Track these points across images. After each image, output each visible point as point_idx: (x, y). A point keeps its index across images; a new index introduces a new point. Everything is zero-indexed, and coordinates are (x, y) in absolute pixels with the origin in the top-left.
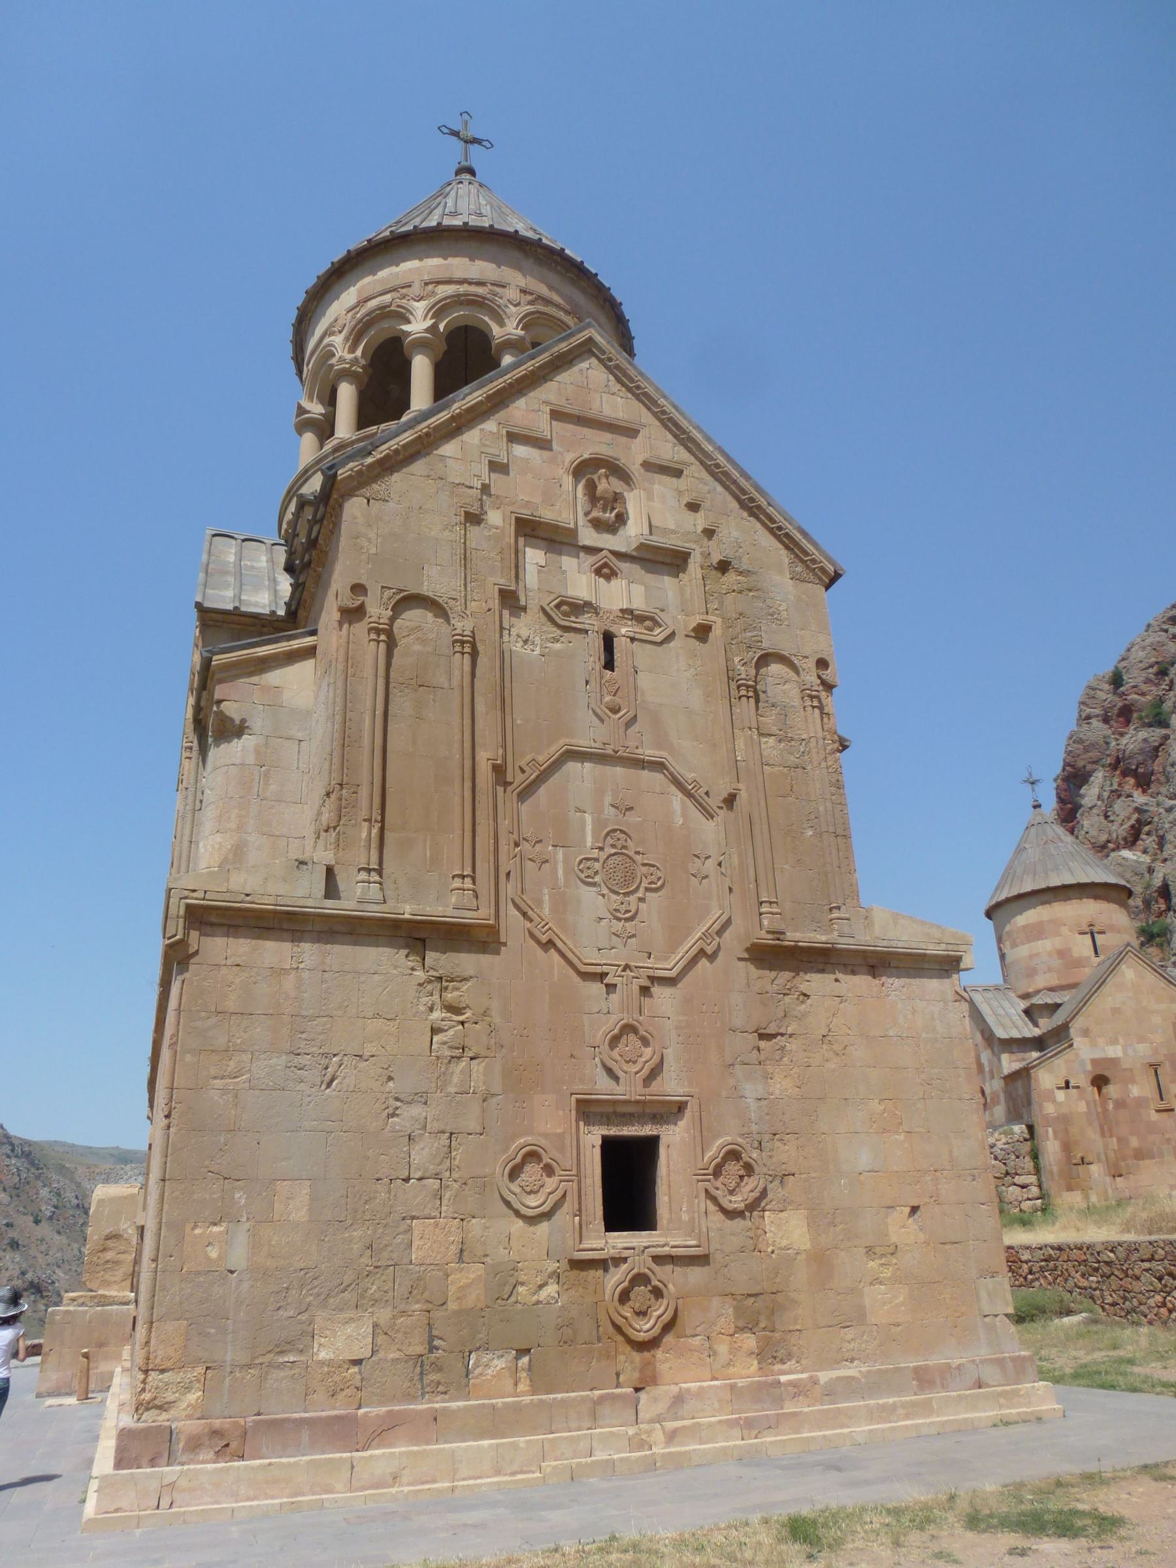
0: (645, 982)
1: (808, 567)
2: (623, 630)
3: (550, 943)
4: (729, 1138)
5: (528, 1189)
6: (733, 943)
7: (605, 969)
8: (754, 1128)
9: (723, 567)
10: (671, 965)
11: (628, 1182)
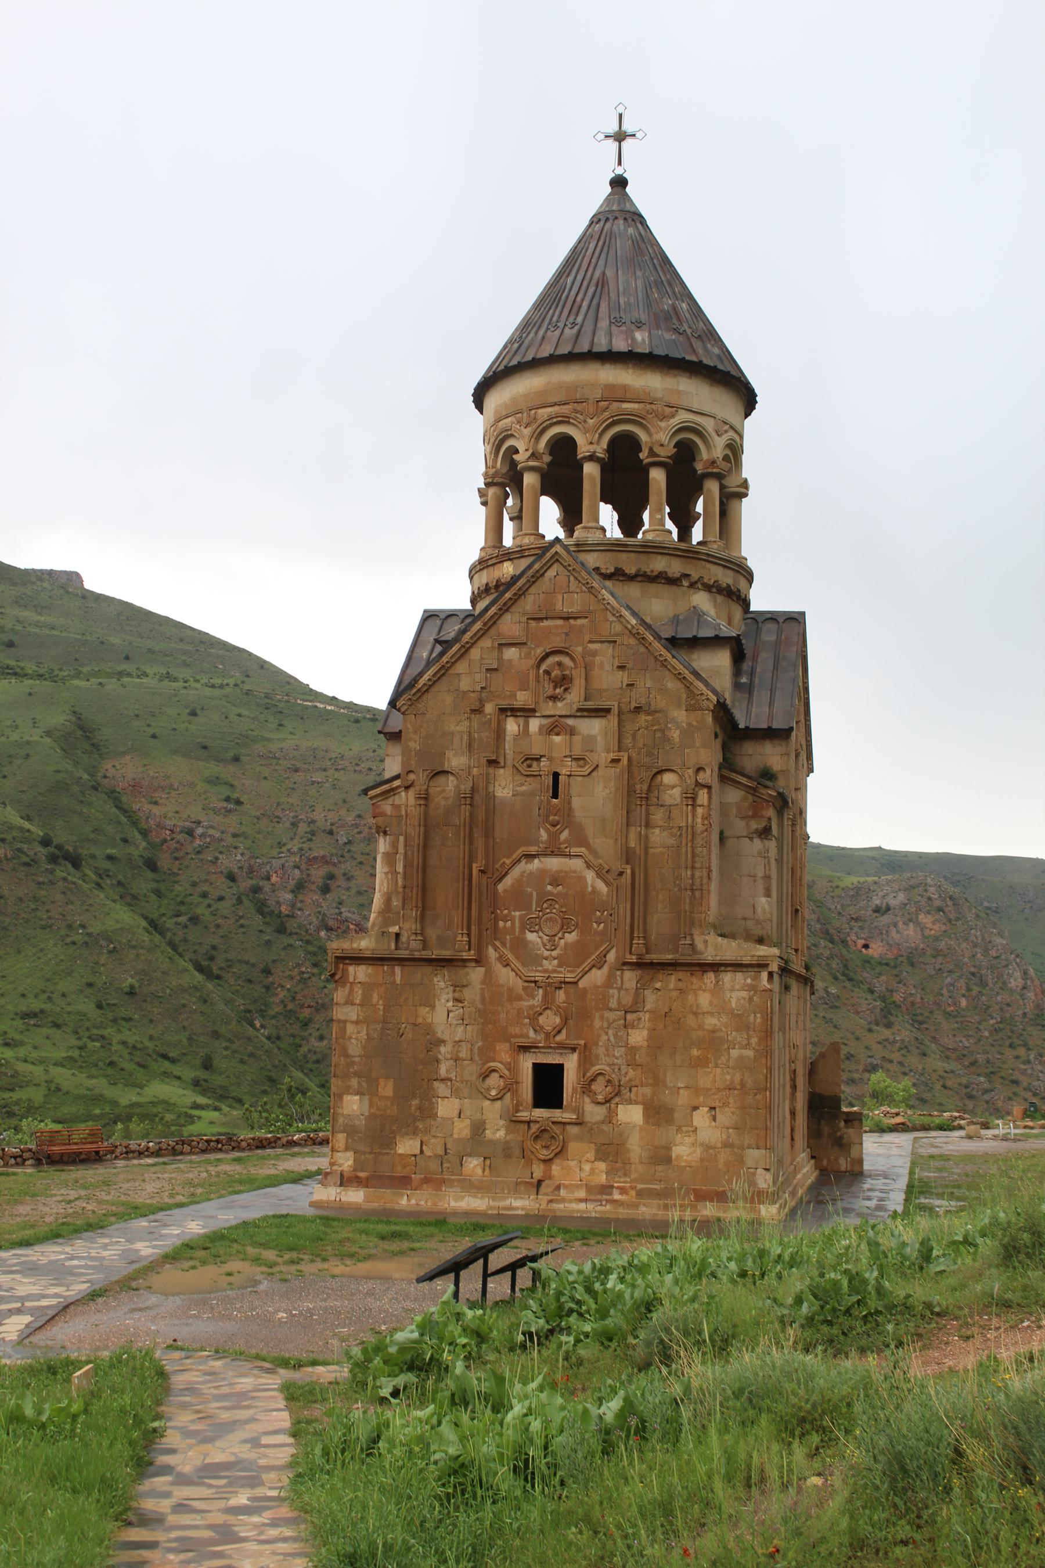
2: (564, 771)
11: (548, 1086)
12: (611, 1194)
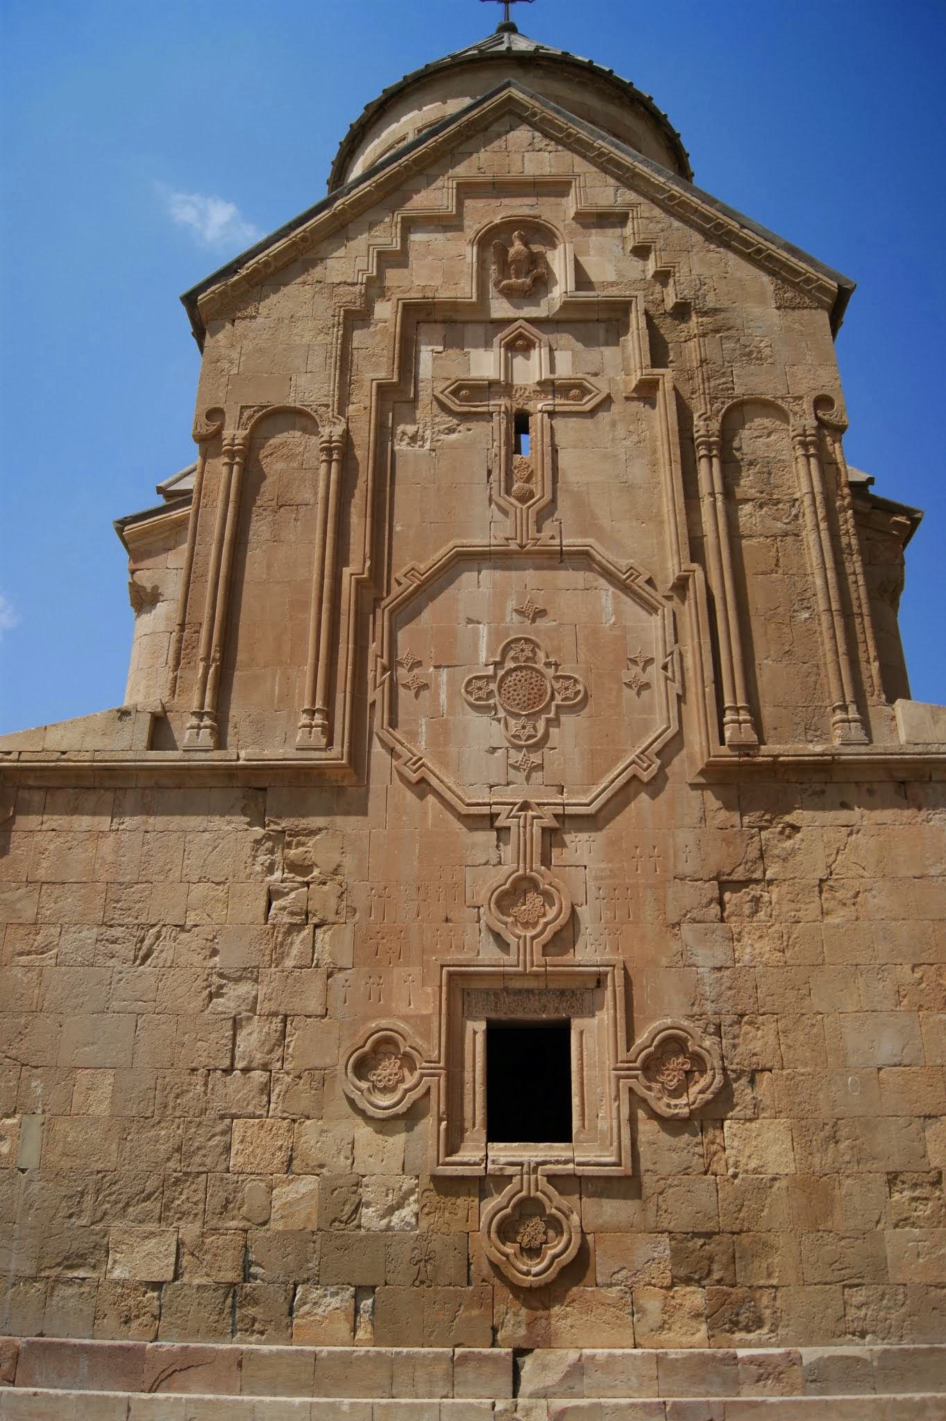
0: (549, 822)
1: (802, 291)
2: (539, 405)
3: (423, 780)
4: (669, 1021)
5: (381, 1085)
6: (687, 765)
7: (495, 809)
8: (709, 1007)
9: (682, 311)
10: (582, 800)
11: (528, 1082)
12: (734, 1384)
